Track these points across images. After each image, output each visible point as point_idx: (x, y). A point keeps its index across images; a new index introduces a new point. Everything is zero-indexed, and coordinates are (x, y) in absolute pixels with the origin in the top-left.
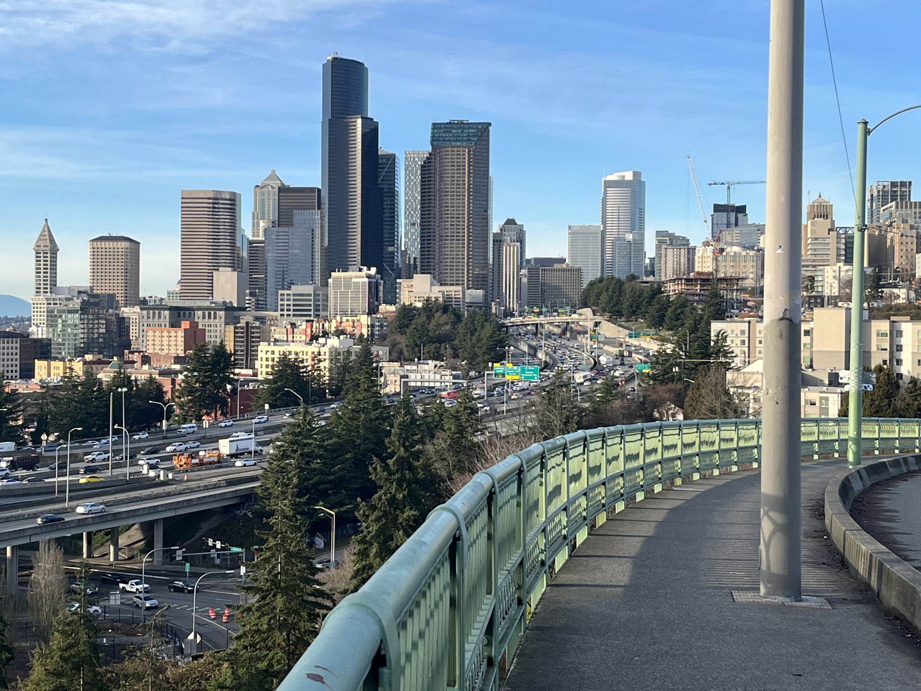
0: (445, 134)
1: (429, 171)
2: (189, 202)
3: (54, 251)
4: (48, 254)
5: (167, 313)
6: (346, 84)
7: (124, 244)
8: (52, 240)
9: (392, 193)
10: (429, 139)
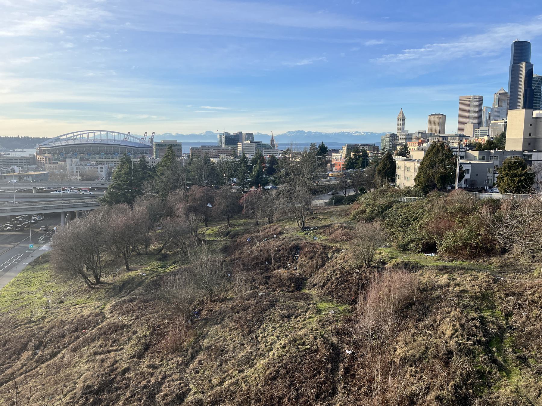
2: (462, 100)
3: (403, 119)
4: (402, 120)
5: (458, 138)
6: (521, 50)
7: (438, 116)
8: (403, 115)
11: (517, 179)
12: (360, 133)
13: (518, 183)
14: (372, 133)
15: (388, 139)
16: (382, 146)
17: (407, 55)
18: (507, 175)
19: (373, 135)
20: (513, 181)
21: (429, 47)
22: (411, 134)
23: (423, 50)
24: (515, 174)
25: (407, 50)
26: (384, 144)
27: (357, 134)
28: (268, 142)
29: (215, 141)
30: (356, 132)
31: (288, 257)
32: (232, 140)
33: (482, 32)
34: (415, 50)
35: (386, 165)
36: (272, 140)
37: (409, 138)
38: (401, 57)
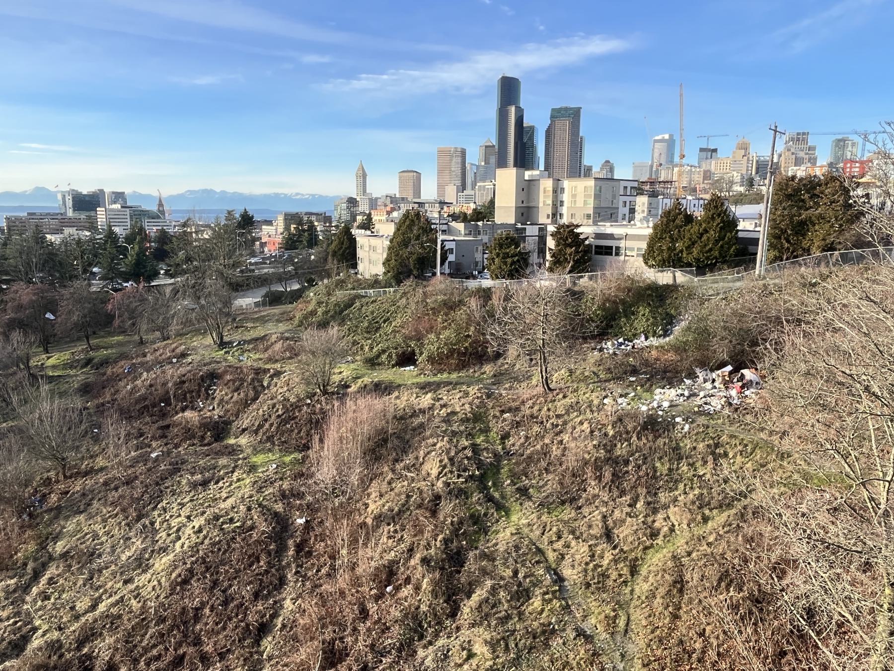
0: (557, 114)
1: (549, 133)
2: (441, 152)
3: (364, 176)
6: (509, 89)
7: (412, 174)
9: (533, 146)
10: (549, 116)
11: (509, 260)
12: (303, 195)
13: (511, 265)
14: (320, 196)
15: (344, 206)
16: (335, 216)
17: (364, 82)
18: (498, 255)
19: (322, 199)
20: (505, 263)
21: (393, 74)
22: (376, 199)
23: (385, 77)
24: (508, 254)
25: (364, 76)
26: (340, 214)
27: (298, 197)
28: (154, 208)
29: (54, 205)
30: (297, 194)
31: (199, 391)
32: (86, 203)
33: (460, 59)
34: (376, 76)
35: (343, 244)
36: (161, 204)
37: (373, 203)
38: (356, 84)
